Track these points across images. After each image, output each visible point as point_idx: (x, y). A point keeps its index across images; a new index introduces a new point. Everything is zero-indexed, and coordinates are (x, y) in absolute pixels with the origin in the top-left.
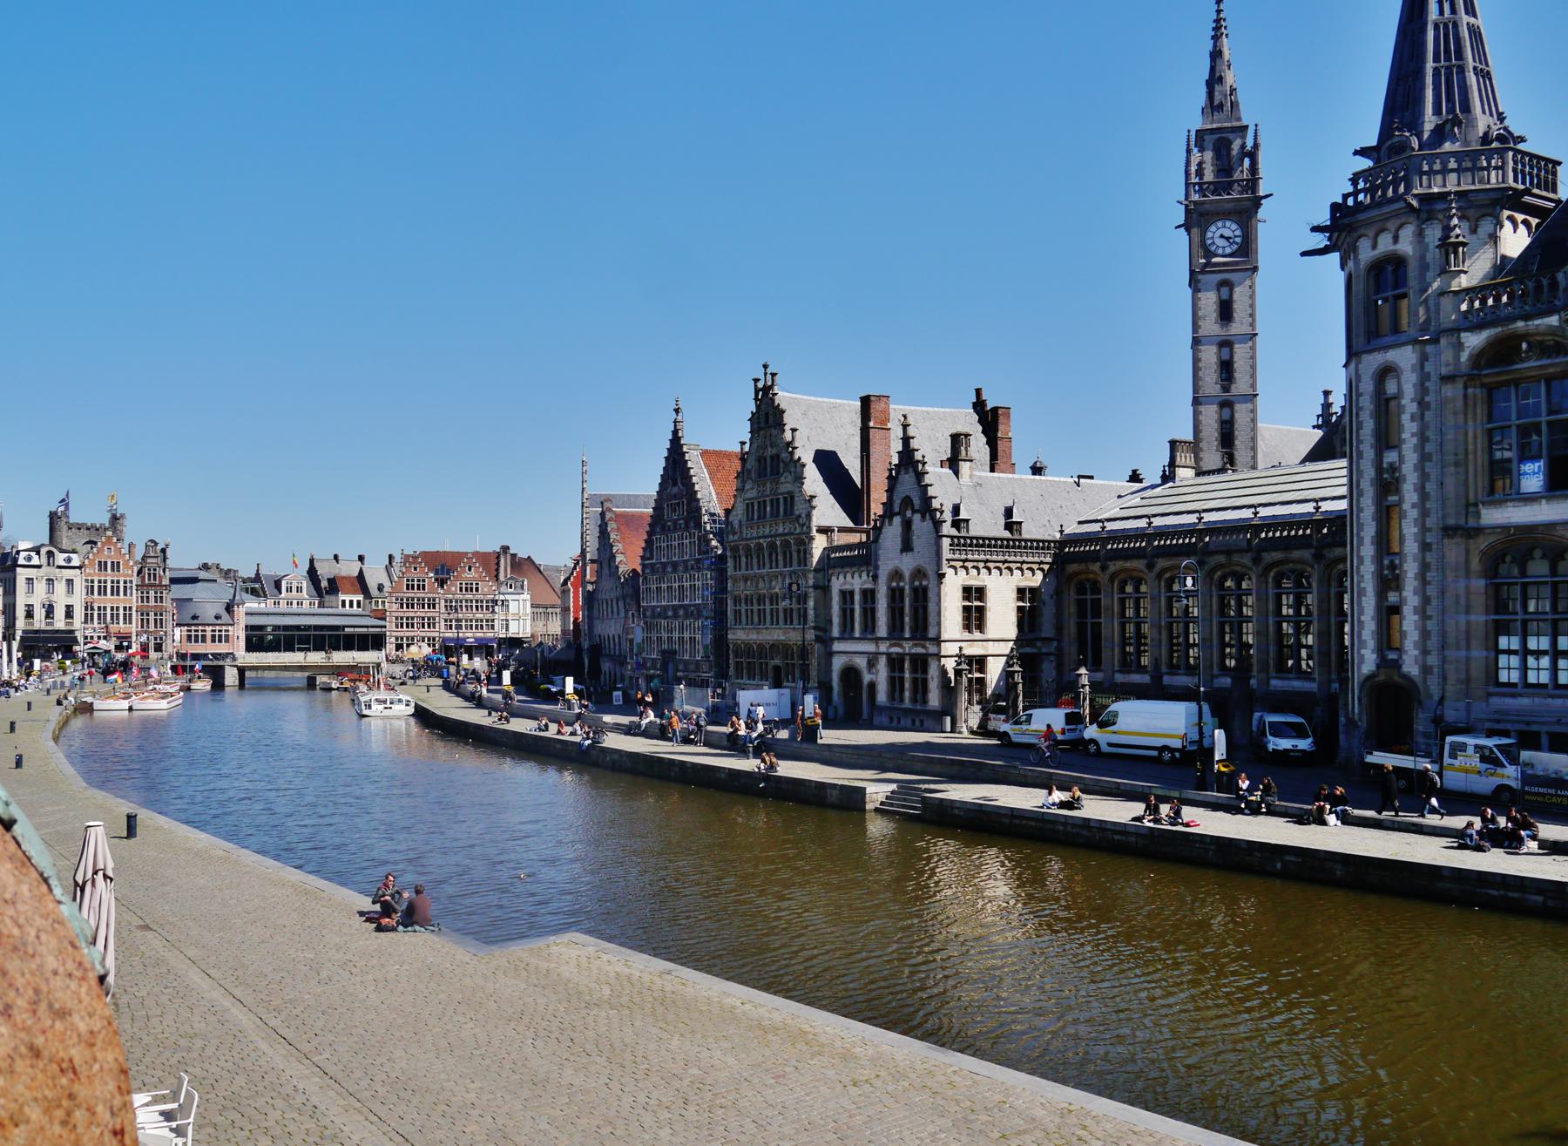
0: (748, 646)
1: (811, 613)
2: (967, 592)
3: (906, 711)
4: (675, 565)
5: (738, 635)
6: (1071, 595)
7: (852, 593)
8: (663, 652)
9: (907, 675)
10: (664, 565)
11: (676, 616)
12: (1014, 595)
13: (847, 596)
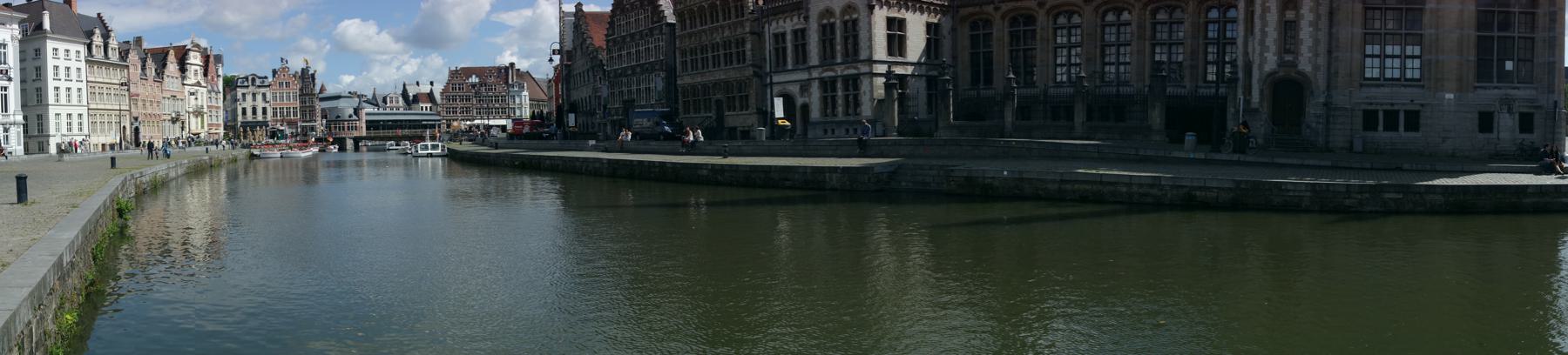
0: (694, 87)
1: (749, 53)
2: (891, 22)
3: (840, 123)
4: (632, 36)
5: (684, 80)
6: (965, 32)
7: (784, 35)
8: (625, 102)
9: (840, 93)
10: (624, 38)
11: (634, 73)
12: (924, 29)
13: (780, 37)
